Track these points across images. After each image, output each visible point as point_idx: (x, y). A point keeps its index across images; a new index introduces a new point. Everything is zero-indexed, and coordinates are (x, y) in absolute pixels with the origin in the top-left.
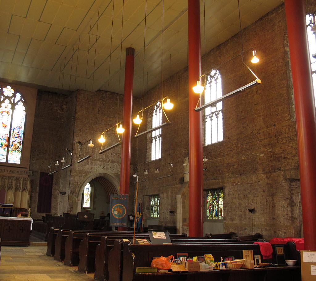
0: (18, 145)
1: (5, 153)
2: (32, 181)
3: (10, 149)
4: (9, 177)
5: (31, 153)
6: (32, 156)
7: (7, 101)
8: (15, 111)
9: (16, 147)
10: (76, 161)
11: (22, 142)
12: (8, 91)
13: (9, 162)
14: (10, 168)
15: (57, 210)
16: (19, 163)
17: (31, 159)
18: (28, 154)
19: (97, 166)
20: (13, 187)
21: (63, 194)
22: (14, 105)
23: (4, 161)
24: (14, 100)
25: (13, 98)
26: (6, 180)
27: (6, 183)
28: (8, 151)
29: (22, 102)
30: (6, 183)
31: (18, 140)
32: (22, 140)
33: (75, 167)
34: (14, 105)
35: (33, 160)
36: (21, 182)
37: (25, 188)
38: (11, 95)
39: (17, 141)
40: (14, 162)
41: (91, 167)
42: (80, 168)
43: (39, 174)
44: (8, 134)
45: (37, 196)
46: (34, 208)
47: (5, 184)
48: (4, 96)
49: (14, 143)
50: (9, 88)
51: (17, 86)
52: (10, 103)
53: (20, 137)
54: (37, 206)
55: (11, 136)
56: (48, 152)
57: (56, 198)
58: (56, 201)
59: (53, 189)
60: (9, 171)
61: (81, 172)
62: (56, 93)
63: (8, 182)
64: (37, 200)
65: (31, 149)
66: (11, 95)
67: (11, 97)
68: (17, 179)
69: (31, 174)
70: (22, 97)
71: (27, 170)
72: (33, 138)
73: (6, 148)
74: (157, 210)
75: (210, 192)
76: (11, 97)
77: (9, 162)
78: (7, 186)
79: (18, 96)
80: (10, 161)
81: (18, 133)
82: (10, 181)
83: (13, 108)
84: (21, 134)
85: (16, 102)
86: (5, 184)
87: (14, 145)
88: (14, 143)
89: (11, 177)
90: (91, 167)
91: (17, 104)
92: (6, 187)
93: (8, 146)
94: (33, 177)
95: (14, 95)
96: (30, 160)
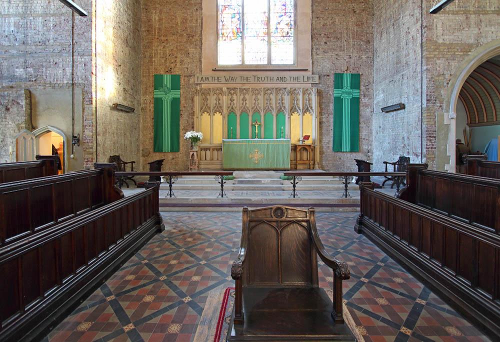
0: (286, 29)
1: (264, 46)
2: (319, 93)
3: (272, 39)
4: (278, 90)
5: (312, 42)
6: (314, 46)
9: (285, 34)
10: (435, 20)
11: (292, 23)
13: (273, 63)
15: (371, 145)
17: (314, 53)
19: (493, 29)
21: (387, 112)
23: (266, 62)
26: (271, 96)
27: (273, 102)
28: (269, 43)
31: (286, 19)
32: (293, 19)
33: (435, 37)
35: (318, 55)
36: (300, 97)
37: (308, 107)
39: (283, 22)
41: (476, 31)
42: (448, 38)
43: (332, 78)
44: (267, 12)
45: (332, 120)
46: (328, 143)
49: (278, 26)
53: (288, 14)
54: (332, 139)
55: (271, 15)
56: (345, 35)
57: (368, 121)
59: (361, 105)
60: (275, 79)
61: (450, 46)
63: (276, 99)
64: (332, 127)
65: (312, 33)
68: (292, 92)
69: (317, 80)
71: (309, 74)
73: (266, 38)
77: (273, 63)
78: (274, 106)
80: (277, 61)
81: (284, 7)
82: (279, 97)
84: (290, 7)
86: (270, 104)
87: (279, 30)
88: (278, 26)
89: (280, 89)
90: (476, 31)
92: (273, 109)
93: (268, 34)
94: (321, 85)
96: (312, 54)
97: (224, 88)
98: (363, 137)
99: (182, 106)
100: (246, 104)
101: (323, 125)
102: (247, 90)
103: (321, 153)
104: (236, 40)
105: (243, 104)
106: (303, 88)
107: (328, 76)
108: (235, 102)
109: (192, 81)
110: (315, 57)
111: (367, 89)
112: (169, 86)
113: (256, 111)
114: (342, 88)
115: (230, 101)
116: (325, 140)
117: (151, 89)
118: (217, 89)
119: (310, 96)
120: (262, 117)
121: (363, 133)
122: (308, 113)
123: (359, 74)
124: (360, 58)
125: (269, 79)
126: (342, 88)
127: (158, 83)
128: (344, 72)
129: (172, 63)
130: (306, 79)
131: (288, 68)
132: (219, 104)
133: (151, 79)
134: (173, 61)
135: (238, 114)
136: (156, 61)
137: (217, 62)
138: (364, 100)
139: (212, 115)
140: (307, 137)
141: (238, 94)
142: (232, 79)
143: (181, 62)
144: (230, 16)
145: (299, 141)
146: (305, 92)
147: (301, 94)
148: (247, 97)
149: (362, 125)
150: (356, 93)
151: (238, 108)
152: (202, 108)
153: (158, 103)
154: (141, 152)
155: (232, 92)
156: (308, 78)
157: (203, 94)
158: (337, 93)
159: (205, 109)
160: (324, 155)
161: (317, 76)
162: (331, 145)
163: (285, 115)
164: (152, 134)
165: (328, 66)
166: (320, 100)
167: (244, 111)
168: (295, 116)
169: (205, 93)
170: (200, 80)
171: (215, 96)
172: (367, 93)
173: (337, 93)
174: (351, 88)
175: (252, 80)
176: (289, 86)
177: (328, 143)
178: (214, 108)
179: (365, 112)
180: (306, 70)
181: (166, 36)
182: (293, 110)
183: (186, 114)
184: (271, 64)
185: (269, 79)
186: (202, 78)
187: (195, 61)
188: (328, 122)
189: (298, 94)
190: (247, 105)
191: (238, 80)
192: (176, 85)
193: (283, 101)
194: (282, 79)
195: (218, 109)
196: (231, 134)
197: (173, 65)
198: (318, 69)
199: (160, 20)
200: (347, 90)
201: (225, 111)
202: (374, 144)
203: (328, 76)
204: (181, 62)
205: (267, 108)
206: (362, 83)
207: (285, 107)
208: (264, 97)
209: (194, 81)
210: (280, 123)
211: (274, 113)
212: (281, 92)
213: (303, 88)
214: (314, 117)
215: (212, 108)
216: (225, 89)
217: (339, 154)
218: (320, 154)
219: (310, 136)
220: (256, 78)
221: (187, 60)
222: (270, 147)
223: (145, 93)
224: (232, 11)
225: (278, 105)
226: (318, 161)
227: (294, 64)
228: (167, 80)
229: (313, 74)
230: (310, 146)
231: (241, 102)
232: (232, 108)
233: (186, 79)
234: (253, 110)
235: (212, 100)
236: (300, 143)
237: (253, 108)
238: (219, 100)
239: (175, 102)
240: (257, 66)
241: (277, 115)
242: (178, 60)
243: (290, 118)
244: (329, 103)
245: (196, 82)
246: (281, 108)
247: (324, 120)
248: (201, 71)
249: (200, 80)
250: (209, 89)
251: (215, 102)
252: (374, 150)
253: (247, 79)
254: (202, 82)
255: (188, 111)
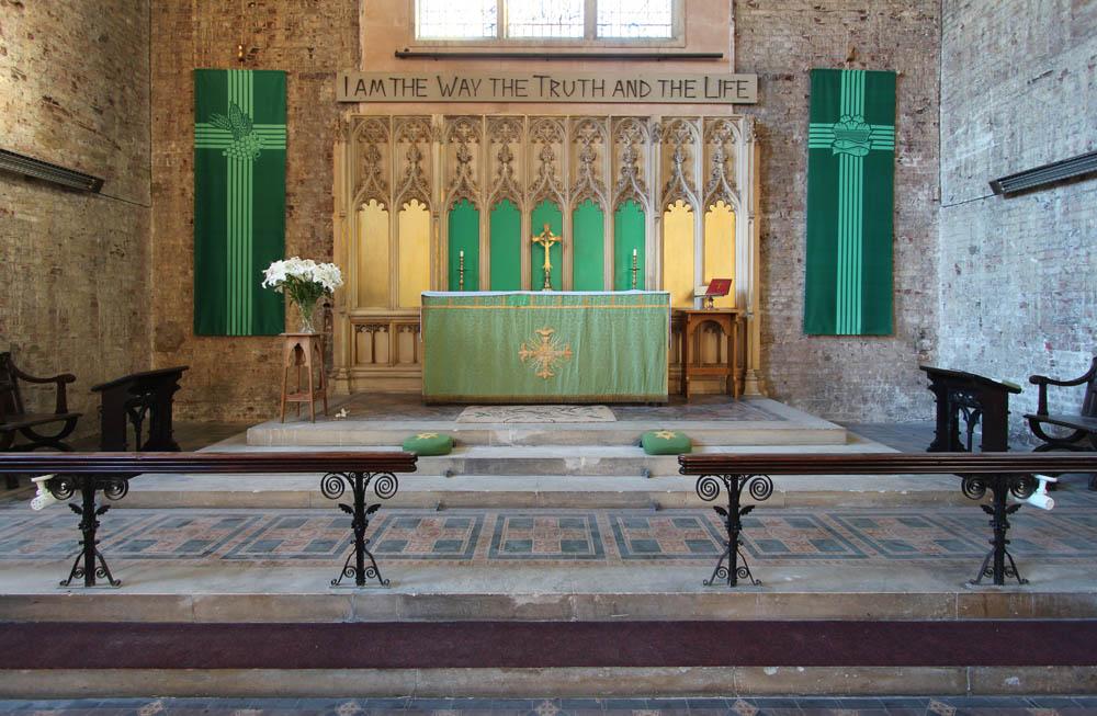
2: (762, 138)
4: (621, 124)
16: (666, 33)
20: (649, 184)
21: (1014, 194)
23: (576, 31)
26: (597, 146)
27: (604, 165)
30: (604, 165)
36: (696, 150)
37: (721, 185)
40: (634, 33)
43: (802, 86)
45: (801, 228)
46: (788, 306)
47: (594, 172)
54: (800, 293)
57: (923, 231)
58: (923, 252)
59: (898, 177)
60: (610, 87)
64: (800, 252)
68: (669, 133)
77: (603, 32)
78: (607, 180)
82: (624, 148)
89: (629, 121)
92: (603, 191)
94: (763, 111)
97: (434, 118)
98: (905, 286)
99: (292, 178)
100: (511, 171)
101: (773, 244)
102: (513, 124)
103: (767, 339)
105: (500, 173)
106: (706, 119)
107: (789, 78)
108: (473, 165)
109: (326, 92)
110: (746, 14)
111: (920, 124)
112: (248, 108)
113: (546, 198)
114: (837, 120)
115: (456, 163)
116: (778, 295)
117: (188, 120)
118: (413, 119)
119: (729, 146)
120: (567, 217)
121: (906, 273)
122: (720, 203)
123: (894, 73)
124: (895, 18)
125: (589, 86)
126: (837, 120)
127: (208, 97)
128: (841, 64)
129: (258, 31)
130: (713, 89)
132: (420, 171)
133: (186, 86)
134: (261, 24)
135: (484, 205)
136: (204, 25)
137: (412, 26)
138: (909, 162)
139: (393, 206)
140: (720, 287)
141: (485, 139)
142: (464, 86)
143: (291, 27)
145: (691, 297)
146: (712, 130)
147: (698, 137)
148: (514, 147)
149: (902, 245)
150: (882, 137)
151: (483, 184)
152: (359, 186)
153: (209, 168)
154: (153, 334)
155: (464, 130)
156: (723, 85)
157: (363, 136)
158: (820, 136)
159: (372, 188)
160: (773, 347)
161: (753, 79)
162: (798, 312)
163: (642, 211)
164: (191, 272)
165: (787, 45)
166: (762, 161)
167: (506, 198)
168: (678, 214)
169: (371, 135)
170: (352, 87)
171: (407, 144)
172: (918, 137)
173: (820, 136)
174: (868, 120)
175: (532, 89)
176: (657, 113)
177: (788, 306)
178: (402, 184)
179: (911, 202)
180: (714, 58)
182: (671, 192)
183: (308, 206)
184: (595, 38)
185: (589, 86)
186: (361, 81)
187: (337, 24)
188: (788, 233)
189: (688, 137)
190: (516, 177)
191: (485, 92)
192: (271, 102)
193: (638, 164)
194: (634, 88)
195: (416, 189)
196: (459, 274)
197: (260, 39)
198: (759, 54)
200: (852, 127)
201: (439, 195)
203: (789, 78)
204: (291, 27)
205: (582, 186)
206: (902, 105)
207: (642, 184)
208: (572, 150)
209: (334, 94)
210: (628, 239)
211: (608, 204)
212: (631, 132)
213: (706, 119)
214: (743, 217)
215: (393, 187)
216: (438, 119)
217: (826, 343)
218: (762, 343)
219: (730, 281)
220: (546, 82)
221: (311, 22)
222: (595, 320)
223: (167, 135)
225: (620, 177)
226: (757, 365)
227: (674, 38)
228: (241, 88)
229: (737, 71)
230: (732, 315)
231: (495, 165)
232: (464, 186)
233: (307, 85)
234: (534, 193)
235: (395, 159)
236: (696, 306)
237: (534, 186)
238: (420, 157)
239: (270, 168)
240: (549, 43)
241: (616, 210)
242: (280, 22)
243: (659, 219)
244: (791, 169)
245: (341, 97)
246: (629, 188)
247: (774, 227)
248: (357, 59)
249: (352, 87)
250: (385, 119)
251: (406, 164)
252: (943, 330)
253: (514, 86)
254: (361, 96)
255: (315, 195)
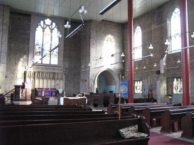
0: (56, 54)
3: (51, 56)
7: (48, 27)
8: (53, 33)
11: (58, 52)
12: (48, 21)
14: (52, 67)
16: (57, 64)
18: (62, 59)
22: (52, 30)
24: (52, 27)
25: (51, 26)
28: (50, 57)
29: (56, 28)
34: (52, 30)
38: (50, 24)
48: (46, 25)
50: (48, 20)
51: (53, 19)
52: (50, 29)
62: (75, 22)
66: (50, 24)
67: (50, 25)
69: (64, 70)
70: (56, 25)
71: (62, 68)
72: (64, 49)
73: (49, 56)
74: (140, 89)
75: (175, 79)
76: (50, 25)
79: (54, 24)
83: (51, 32)
85: (53, 28)
91: (53, 29)
95: (52, 24)
104: (40, 56)
131: (56, 66)
144: (38, 48)
181: (16, 52)
191: (40, 69)
199: (14, 46)
202: (81, 90)
224: (39, 46)
227: (58, 65)
